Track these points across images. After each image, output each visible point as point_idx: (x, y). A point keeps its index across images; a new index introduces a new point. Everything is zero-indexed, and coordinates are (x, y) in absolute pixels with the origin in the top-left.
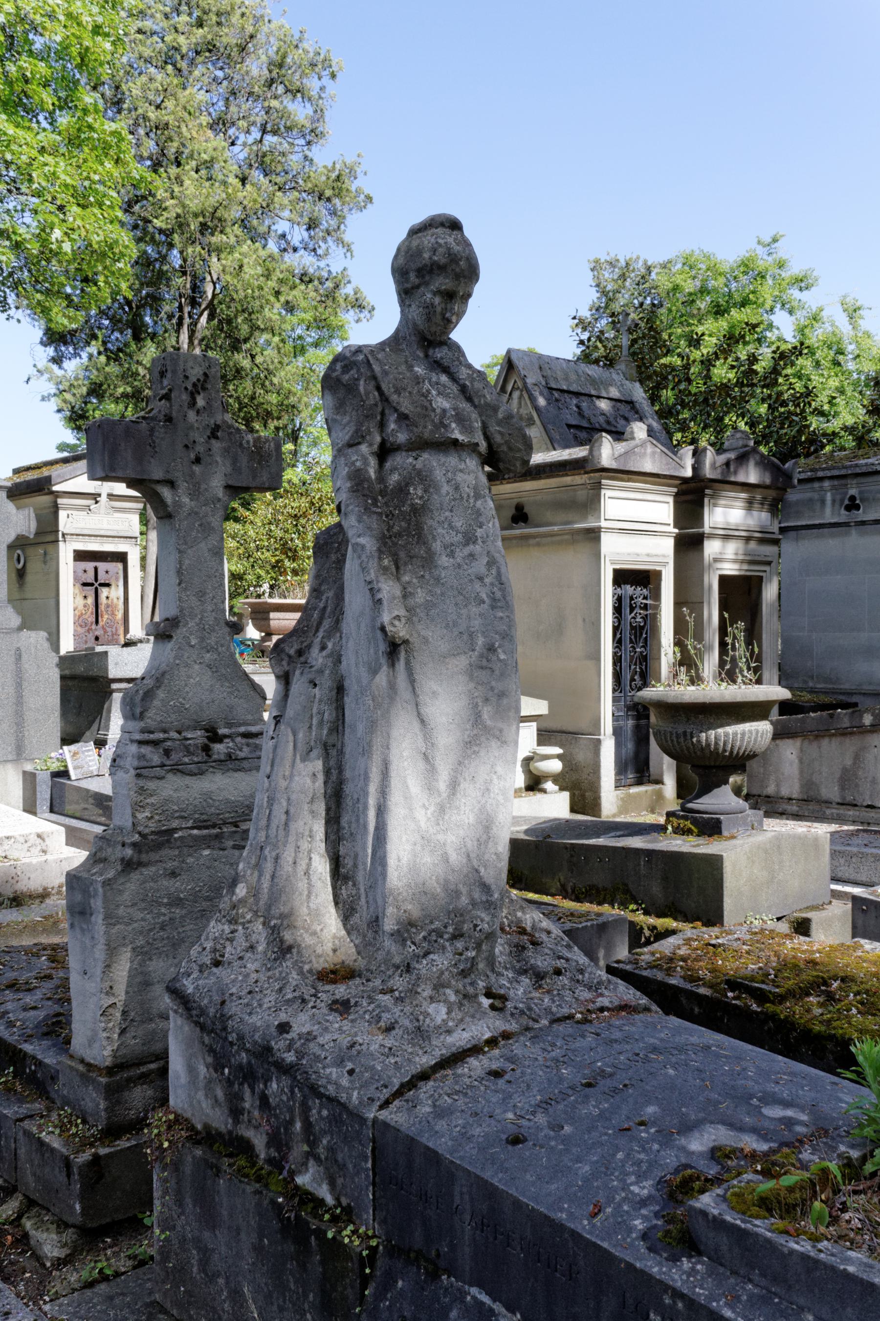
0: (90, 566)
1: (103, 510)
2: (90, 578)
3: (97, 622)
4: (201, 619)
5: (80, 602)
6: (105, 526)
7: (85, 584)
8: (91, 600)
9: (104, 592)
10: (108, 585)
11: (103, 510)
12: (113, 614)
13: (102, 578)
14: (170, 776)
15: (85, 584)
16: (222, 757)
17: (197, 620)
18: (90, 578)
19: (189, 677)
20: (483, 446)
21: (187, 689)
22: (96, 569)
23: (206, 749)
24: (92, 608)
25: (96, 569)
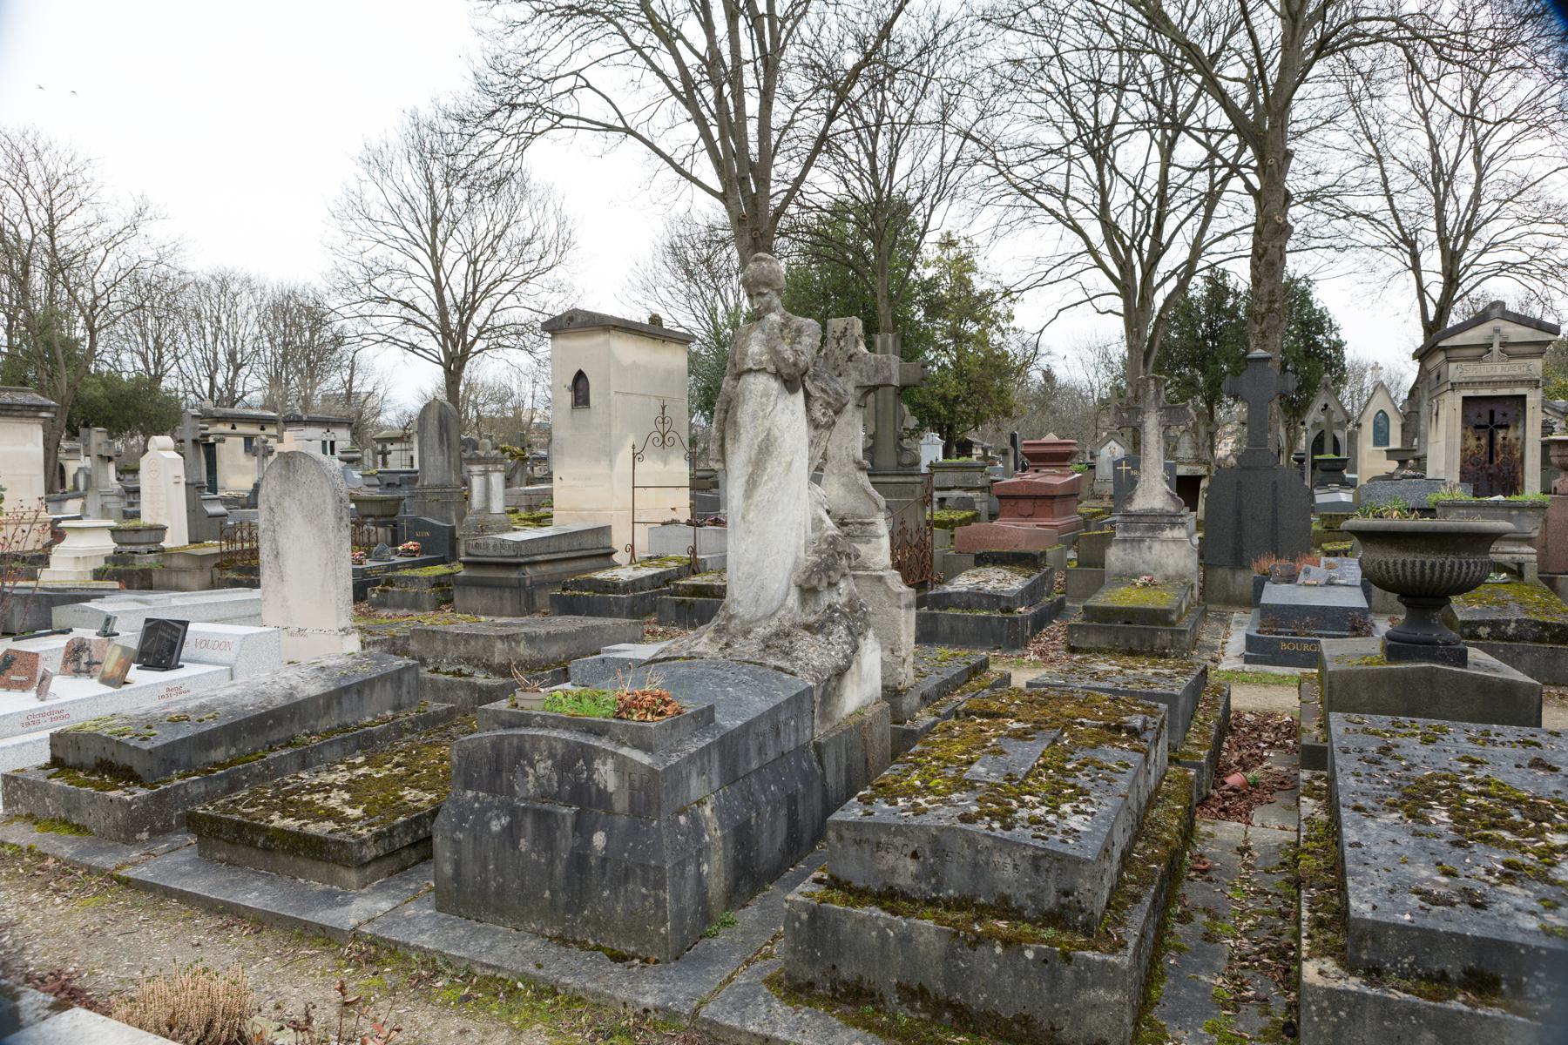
0: (1485, 410)
1: (1495, 358)
2: (1485, 420)
3: (1491, 461)
5: (1472, 443)
6: (1499, 372)
7: (1477, 427)
8: (1483, 442)
9: (1501, 434)
10: (1507, 427)
11: (1495, 358)
12: (1510, 453)
13: (1498, 419)
15: (1477, 427)
18: (1485, 420)
20: (772, 368)
22: (1492, 413)
24: (1485, 449)
25: (1492, 413)
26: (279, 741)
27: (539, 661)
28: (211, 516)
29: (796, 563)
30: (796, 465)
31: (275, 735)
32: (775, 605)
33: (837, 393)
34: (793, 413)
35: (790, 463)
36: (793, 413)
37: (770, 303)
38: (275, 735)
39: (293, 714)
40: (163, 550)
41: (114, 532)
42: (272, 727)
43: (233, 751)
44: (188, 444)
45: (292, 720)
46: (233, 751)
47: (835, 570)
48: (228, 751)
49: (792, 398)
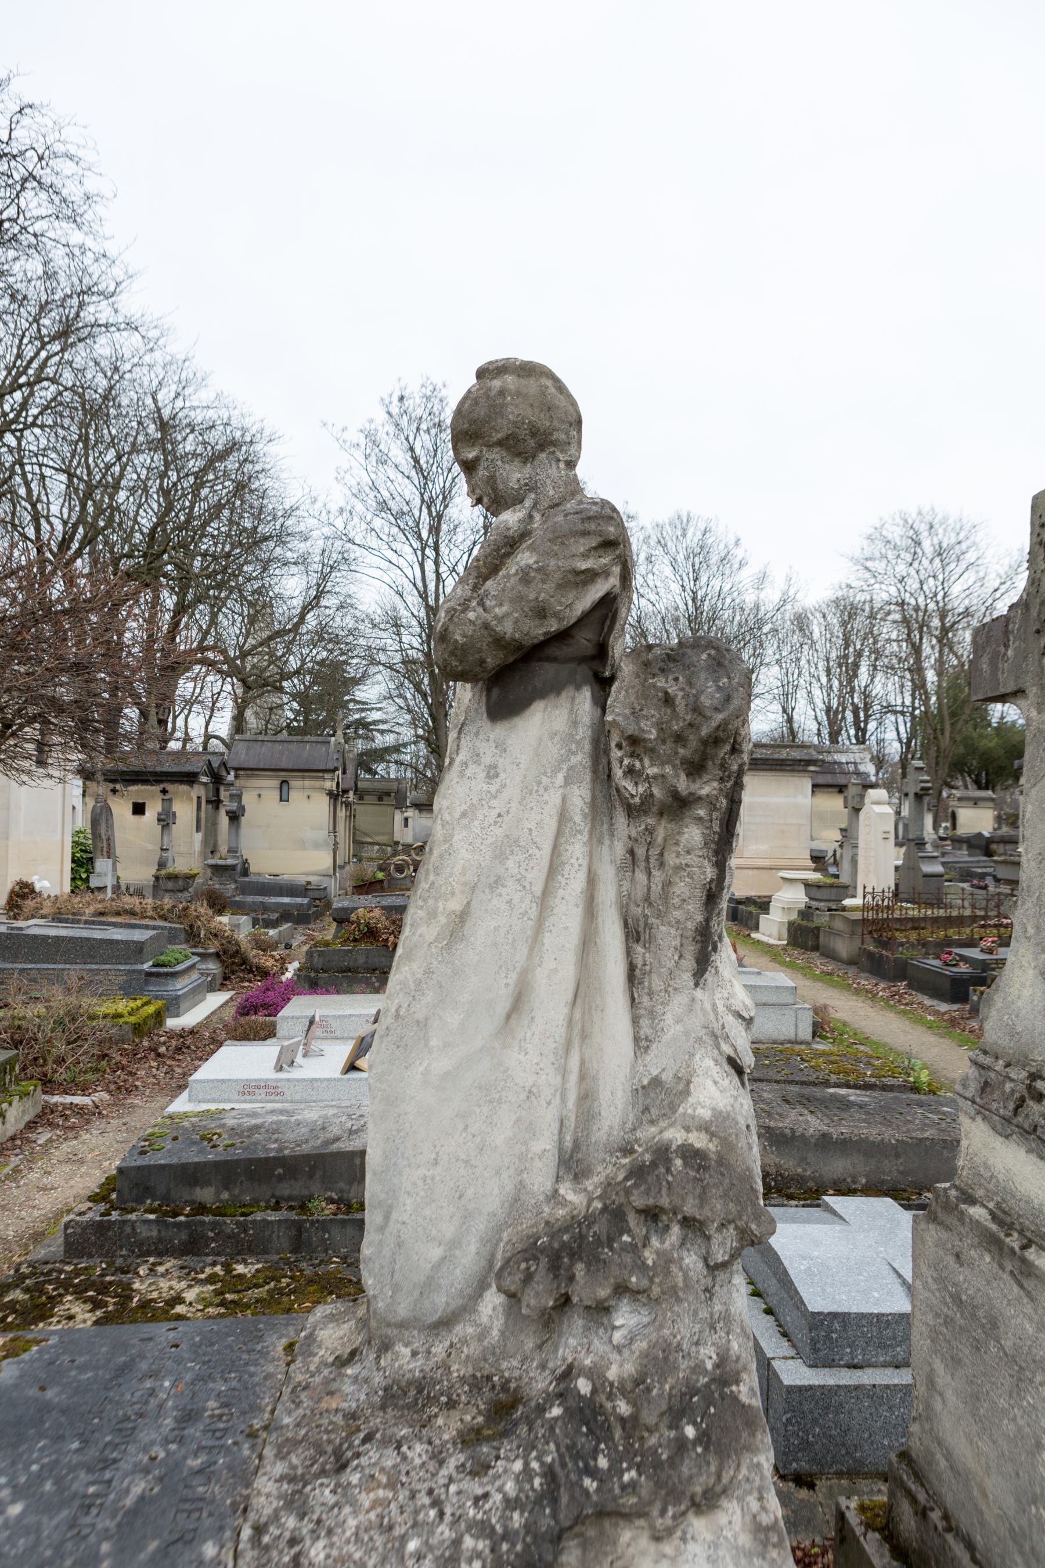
4: (1038, 898)
14: (979, 1119)
16: (1026, 1126)
17: (1034, 899)
19: (1023, 985)
21: (1020, 1004)
23: (1021, 1103)
26: (290, 1198)
27: (800, 1180)
28: (926, 876)
29: (516, 1201)
30: (499, 920)
31: (285, 1189)
32: (441, 1302)
33: (696, 709)
34: (492, 772)
35: (463, 916)
36: (492, 772)
37: (492, 480)
38: (285, 1189)
39: (313, 1169)
40: (844, 909)
41: (807, 885)
42: (280, 1179)
43: (225, 1196)
44: (911, 796)
45: (311, 1176)
46: (225, 1196)
47: (595, 1263)
48: (218, 1193)
49: (499, 730)
